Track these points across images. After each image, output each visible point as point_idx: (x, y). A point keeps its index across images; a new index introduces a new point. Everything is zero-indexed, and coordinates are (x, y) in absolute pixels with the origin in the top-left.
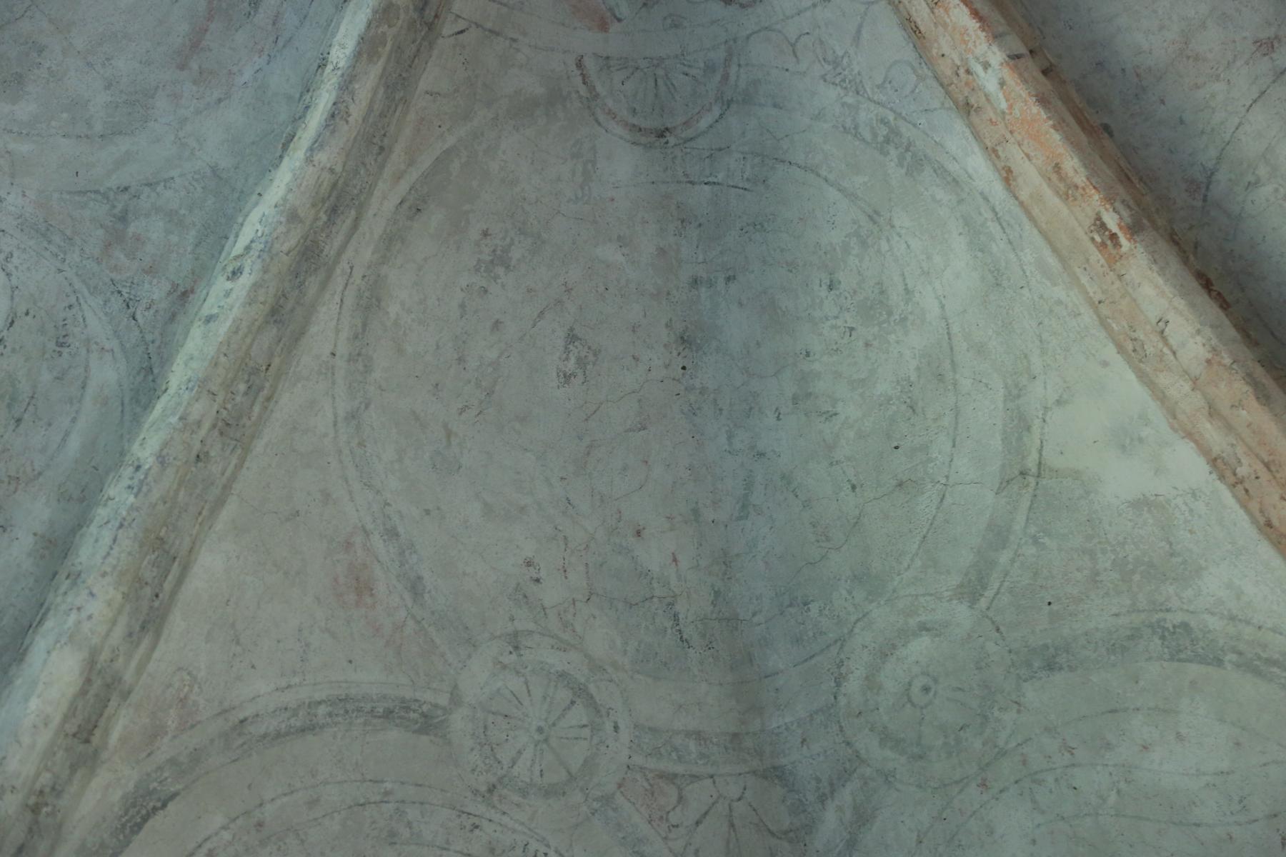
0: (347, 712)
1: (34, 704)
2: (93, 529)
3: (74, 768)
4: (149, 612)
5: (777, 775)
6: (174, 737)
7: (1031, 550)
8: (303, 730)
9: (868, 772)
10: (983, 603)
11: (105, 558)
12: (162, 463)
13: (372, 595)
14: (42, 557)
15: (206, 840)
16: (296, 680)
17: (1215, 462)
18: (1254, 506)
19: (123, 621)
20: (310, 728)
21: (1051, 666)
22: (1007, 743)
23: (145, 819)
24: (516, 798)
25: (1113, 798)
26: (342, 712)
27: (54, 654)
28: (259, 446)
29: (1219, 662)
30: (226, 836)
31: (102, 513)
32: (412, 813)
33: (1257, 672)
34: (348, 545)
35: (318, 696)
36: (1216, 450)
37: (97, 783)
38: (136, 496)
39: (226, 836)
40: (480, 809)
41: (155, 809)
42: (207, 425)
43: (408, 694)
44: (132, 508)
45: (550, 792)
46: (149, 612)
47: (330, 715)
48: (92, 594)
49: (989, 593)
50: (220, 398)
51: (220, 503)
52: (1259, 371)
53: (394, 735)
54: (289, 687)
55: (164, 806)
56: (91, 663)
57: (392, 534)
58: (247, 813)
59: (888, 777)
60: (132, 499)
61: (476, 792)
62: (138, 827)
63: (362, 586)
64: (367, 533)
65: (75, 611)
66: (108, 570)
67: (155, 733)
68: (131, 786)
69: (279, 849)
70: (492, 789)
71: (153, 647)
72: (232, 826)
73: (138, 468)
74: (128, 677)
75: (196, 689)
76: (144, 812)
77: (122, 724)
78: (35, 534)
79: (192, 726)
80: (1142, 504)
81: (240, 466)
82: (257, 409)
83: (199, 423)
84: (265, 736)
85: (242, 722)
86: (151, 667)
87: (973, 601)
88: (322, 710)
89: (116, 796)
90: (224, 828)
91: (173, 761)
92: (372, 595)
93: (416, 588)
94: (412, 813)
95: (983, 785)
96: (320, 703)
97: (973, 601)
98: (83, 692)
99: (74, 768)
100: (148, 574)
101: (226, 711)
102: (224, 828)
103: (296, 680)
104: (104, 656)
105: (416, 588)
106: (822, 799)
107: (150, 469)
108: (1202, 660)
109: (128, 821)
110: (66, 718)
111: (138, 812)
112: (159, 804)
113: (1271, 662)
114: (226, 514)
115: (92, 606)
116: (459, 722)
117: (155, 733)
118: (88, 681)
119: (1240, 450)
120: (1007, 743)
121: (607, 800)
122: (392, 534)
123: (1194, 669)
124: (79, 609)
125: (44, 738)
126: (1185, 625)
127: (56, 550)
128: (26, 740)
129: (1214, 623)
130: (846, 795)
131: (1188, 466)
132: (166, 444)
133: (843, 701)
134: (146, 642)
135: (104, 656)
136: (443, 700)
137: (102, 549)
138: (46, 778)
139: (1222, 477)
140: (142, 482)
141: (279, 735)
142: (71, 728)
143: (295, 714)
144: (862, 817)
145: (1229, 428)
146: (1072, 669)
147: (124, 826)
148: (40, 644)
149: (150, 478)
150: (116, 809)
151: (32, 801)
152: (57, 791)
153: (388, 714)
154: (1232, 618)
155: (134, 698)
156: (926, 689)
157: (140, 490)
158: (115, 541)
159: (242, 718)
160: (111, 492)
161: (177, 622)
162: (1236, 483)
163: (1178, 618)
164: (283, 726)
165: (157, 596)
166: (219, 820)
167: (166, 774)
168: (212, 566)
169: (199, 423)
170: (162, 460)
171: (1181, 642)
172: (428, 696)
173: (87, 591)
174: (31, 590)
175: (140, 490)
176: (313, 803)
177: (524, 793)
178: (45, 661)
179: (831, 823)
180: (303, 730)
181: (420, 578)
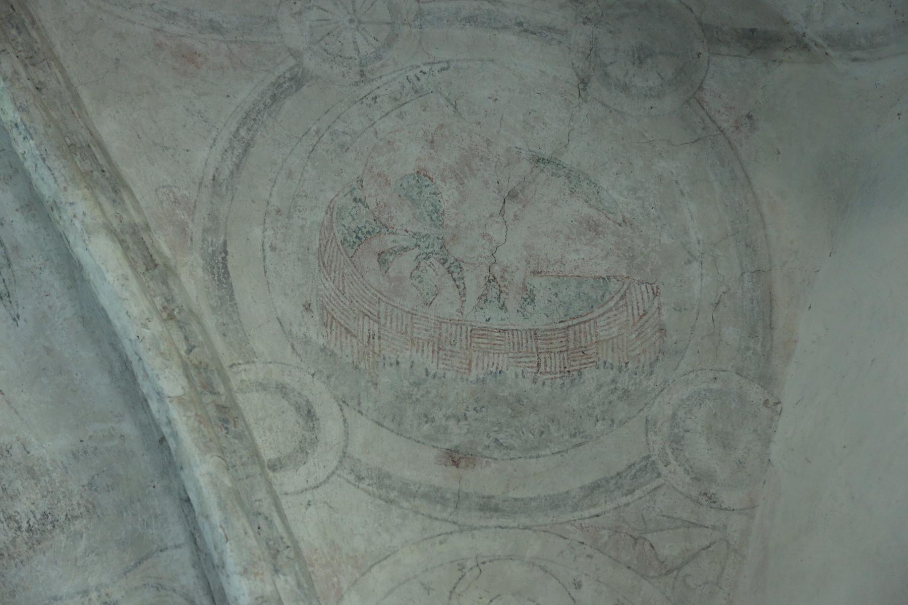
0: (255, 120)
1: (110, 277)
2: (35, 176)
3: (165, 282)
4: (108, 181)
6: (193, 220)
8: (245, 151)
11: (56, 182)
12: (23, 110)
13: (199, 55)
14: (34, 216)
15: (263, 245)
16: (214, 133)
19: (102, 199)
20: (247, 147)
23: (225, 267)
24: (378, 64)
26: (252, 122)
27: (90, 247)
28: (59, 50)
30: (270, 232)
31: (28, 164)
32: (339, 127)
34: (159, 46)
35: (233, 129)
37: (184, 278)
38: (32, 139)
39: (270, 232)
40: (368, 88)
41: (224, 259)
42: (21, 69)
43: (272, 78)
44: (38, 146)
45: (389, 43)
46: (108, 181)
47: (249, 130)
48: (72, 204)
50: (10, 49)
51: (76, 97)
53: (288, 104)
54: (215, 140)
55: (226, 253)
56: (113, 233)
57: (172, 16)
58: (267, 213)
60: (32, 142)
61: (356, 84)
62: (227, 272)
63: (190, 57)
64: (159, 30)
65: (74, 220)
66: (64, 185)
67: (183, 229)
68: (201, 261)
69: (300, 211)
70: (362, 74)
71: (132, 195)
72: (267, 226)
73: (16, 125)
74: (137, 219)
75: (175, 190)
76: (221, 265)
77: (163, 243)
78: (17, 210)
79: (195, 207)
81: (63, 71)
82: (34, 34)
83: (16, 72)
84: (232, 173)
85: (214, 180)
86: (143, 204)
88: (243, 132)
89: (200, 272)
90: (265, 230)
91: (206, 231)
92: (199, 55)
93: (214, 27)
94: (339, 127)
96: (238, 130)
98: (126, 249)
99: (165, 282)
100: (87, 166)
101: (200, 184)
102: (265, 230)
103: (214, 133)
104: (115, 223)
105: (214, 27)
107: (21, 119)
109: (219, 275)
110: (133, 267)
111: (219, 268)
112: (223, 255)
114: (86, 96)
115: (79, 208)
116: (310, 63)
117: (183, 229)
118: (122, 242)
121: (420, 14)
122: (172, 16)
124: (75, 216)
125: (134, 285)
127: (35, 206)
128: (126, 294)
132: (14, 100)
134: (125, 196)
135: (115, 223)
136: (291, 62)
137: (51, 179)
138: (159, 301)
140: (26, 130)
141: (237, 166)
142: (141, 268)
143: (234, 148)
147: (219, 280)
148: (79, 250)
149: (28, 124)
150: (207, 278)
151: (165, 315)
152: (170, 300)
153: (274, 98)
155: (153, 225)
157: (30, 134)
158: (50, 169)
159: (211, 178)
160: (20, 151)
161: (128, 172)
164: (234, 159)
165: (103, 171)
166: (257, 231)
167: (210, 240)
168: (110, 128)
169: (16, 72)
170: (21, 109)
172: (282, 68)
173: (68, 205)
174: (48, 235)
175: (30, 134)
176: (290, 175)
177: (378, 57)
178: (91, 255)
180: (245, 151)
181: (211, 21)
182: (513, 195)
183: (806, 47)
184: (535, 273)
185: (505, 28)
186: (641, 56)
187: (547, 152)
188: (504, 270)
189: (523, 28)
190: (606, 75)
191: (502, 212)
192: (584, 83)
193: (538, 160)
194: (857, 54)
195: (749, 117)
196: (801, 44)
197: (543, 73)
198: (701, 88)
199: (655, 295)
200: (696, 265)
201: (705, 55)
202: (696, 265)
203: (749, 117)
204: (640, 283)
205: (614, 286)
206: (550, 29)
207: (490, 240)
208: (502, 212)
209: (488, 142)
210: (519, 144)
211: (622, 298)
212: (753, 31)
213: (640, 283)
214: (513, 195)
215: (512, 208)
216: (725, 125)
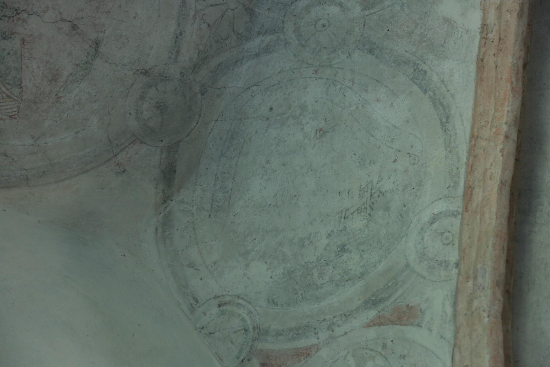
5: (251, 13)
7: (398, 8)
9: (282, 37)
10: (367, 12)
17: (484, 26)
18: (483, 50)
21: (370, 51)
22: (335, 64)
25: (354, 108)
29: (425, 92)
33: (434, 104)
36: (488, 22)
49: (372, 11)
52: (526, 6)
59: (287, 44)
80: (448, 21)
87: (364, 9)
95: (316, 72)
97: (364, 9)
106: (259, 33)
108: (421, 88)
113: (441, 104)
119: (496, 28)
120: (335, 64)
123: (416, 88)
126: (425, 72)
129: (435, 78)
130: (268, 39)
131: (474, 20)
133: (293, 7)
139: (481, 33)
144: (268, 50)
145: (499, 17)
146: (377, 57)
154: (442, 81)
156: (324, 26)
162: (484, 38)
163: (425, 68)
171: (420, 77)
179: (255, 44)
182: (74, 27)
183: (165, 202)
184: (23, 40)
185: (179, 25)
186: (161, 107)
187: (103, 49)
188: (24, 20)
189: (178, 36)
190: (150, 87)
191: (63, 20)
192: (146, 73)
193: (97, 44)
194: (160, 230)
195: (124, 171)
196: (166, 199)
197: (152, 48)
198: (142, 142)
199: (11, 117)
200: (31, 142)
201: (161, 145)
202: (31, 142)
203: (124, 171)
204: (19, 107)
205: (16, 91)
206: (178, 52)
207: (45, 12)
208: (63, 20)
209: (108, 12)
210: (107, 32)
211: (8, 96)
212: (175, 171)
213: (19, 107)
214: (74, 27)
215: (66, 26)
216: (119, 157)
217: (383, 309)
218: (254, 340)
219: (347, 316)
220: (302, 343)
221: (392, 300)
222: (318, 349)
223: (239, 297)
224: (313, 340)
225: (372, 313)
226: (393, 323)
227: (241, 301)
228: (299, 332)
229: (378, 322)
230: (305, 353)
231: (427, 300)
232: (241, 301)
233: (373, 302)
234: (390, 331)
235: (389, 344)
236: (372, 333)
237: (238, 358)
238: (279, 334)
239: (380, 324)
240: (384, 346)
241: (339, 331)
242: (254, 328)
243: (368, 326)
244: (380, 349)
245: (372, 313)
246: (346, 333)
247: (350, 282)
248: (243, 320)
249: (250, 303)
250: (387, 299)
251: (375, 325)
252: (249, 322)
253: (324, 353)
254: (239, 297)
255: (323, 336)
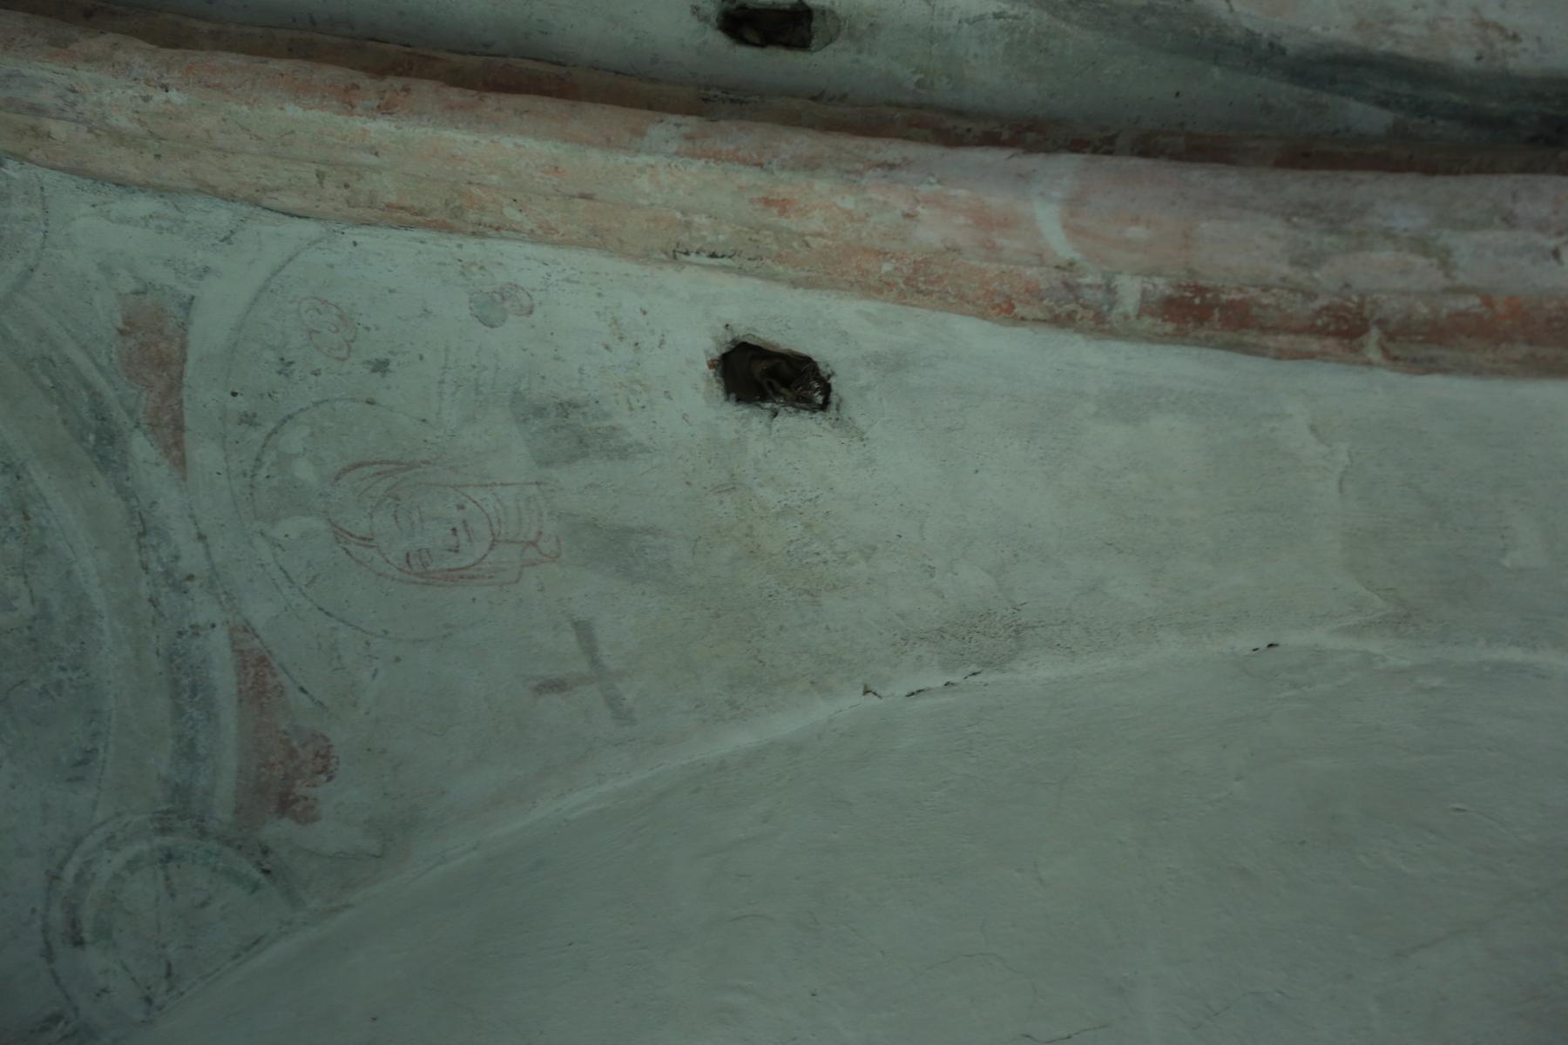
217: (131, 412)
218: (204, 834)
219: (144, 528)
220: (224, 679)
221: (101, 383)
222: (248, 628)
223: (54, 878)
224: (218, 645)
225: (141, 447)
226: (175, 385)
227: (70, 871)
228: (185, 684)
229: (171, 433)
230: (258, 672)
231: (105, 268)
232: (70, 871)
233: (105, 444)
234: (203, 396)
235: (242, 404)
236: (204, 454)
237: (256, 887)
238: (188, 752)
239: (178, 426)
240: (249, 420)
241: (192, 559)
242: (163, 831)
243: (181, 463)
244: (256, 436)
245: (141, 447)
246: (201, 537)
247: (33, 509)
248: (133, 865)
249: (78, 841)
250: (95, 395)
251: (178, 444)
252: (141, 847)
253: (260, 612)
254: (54, 878)
255: (204, 609)
